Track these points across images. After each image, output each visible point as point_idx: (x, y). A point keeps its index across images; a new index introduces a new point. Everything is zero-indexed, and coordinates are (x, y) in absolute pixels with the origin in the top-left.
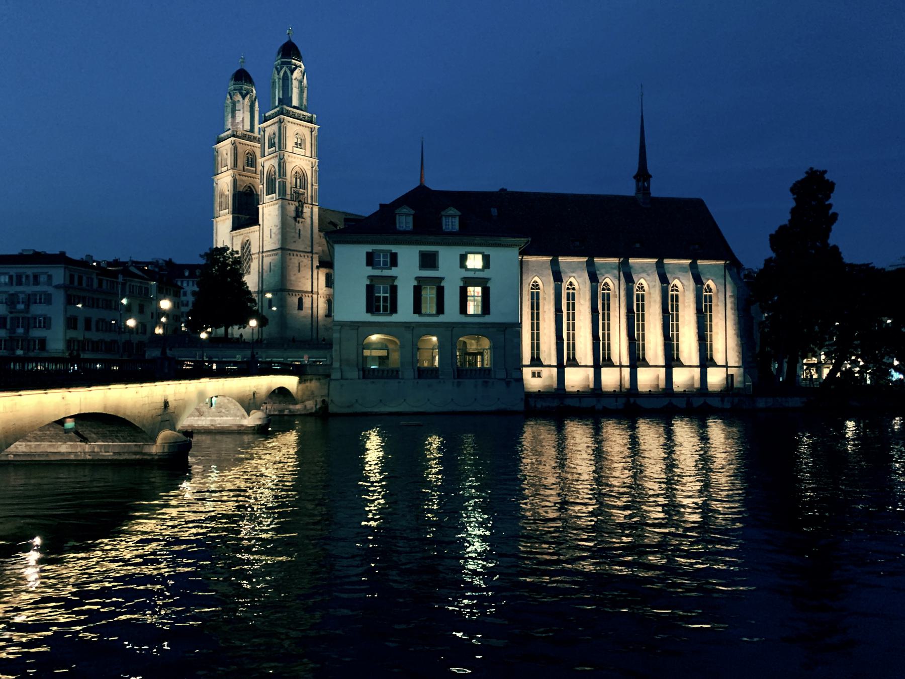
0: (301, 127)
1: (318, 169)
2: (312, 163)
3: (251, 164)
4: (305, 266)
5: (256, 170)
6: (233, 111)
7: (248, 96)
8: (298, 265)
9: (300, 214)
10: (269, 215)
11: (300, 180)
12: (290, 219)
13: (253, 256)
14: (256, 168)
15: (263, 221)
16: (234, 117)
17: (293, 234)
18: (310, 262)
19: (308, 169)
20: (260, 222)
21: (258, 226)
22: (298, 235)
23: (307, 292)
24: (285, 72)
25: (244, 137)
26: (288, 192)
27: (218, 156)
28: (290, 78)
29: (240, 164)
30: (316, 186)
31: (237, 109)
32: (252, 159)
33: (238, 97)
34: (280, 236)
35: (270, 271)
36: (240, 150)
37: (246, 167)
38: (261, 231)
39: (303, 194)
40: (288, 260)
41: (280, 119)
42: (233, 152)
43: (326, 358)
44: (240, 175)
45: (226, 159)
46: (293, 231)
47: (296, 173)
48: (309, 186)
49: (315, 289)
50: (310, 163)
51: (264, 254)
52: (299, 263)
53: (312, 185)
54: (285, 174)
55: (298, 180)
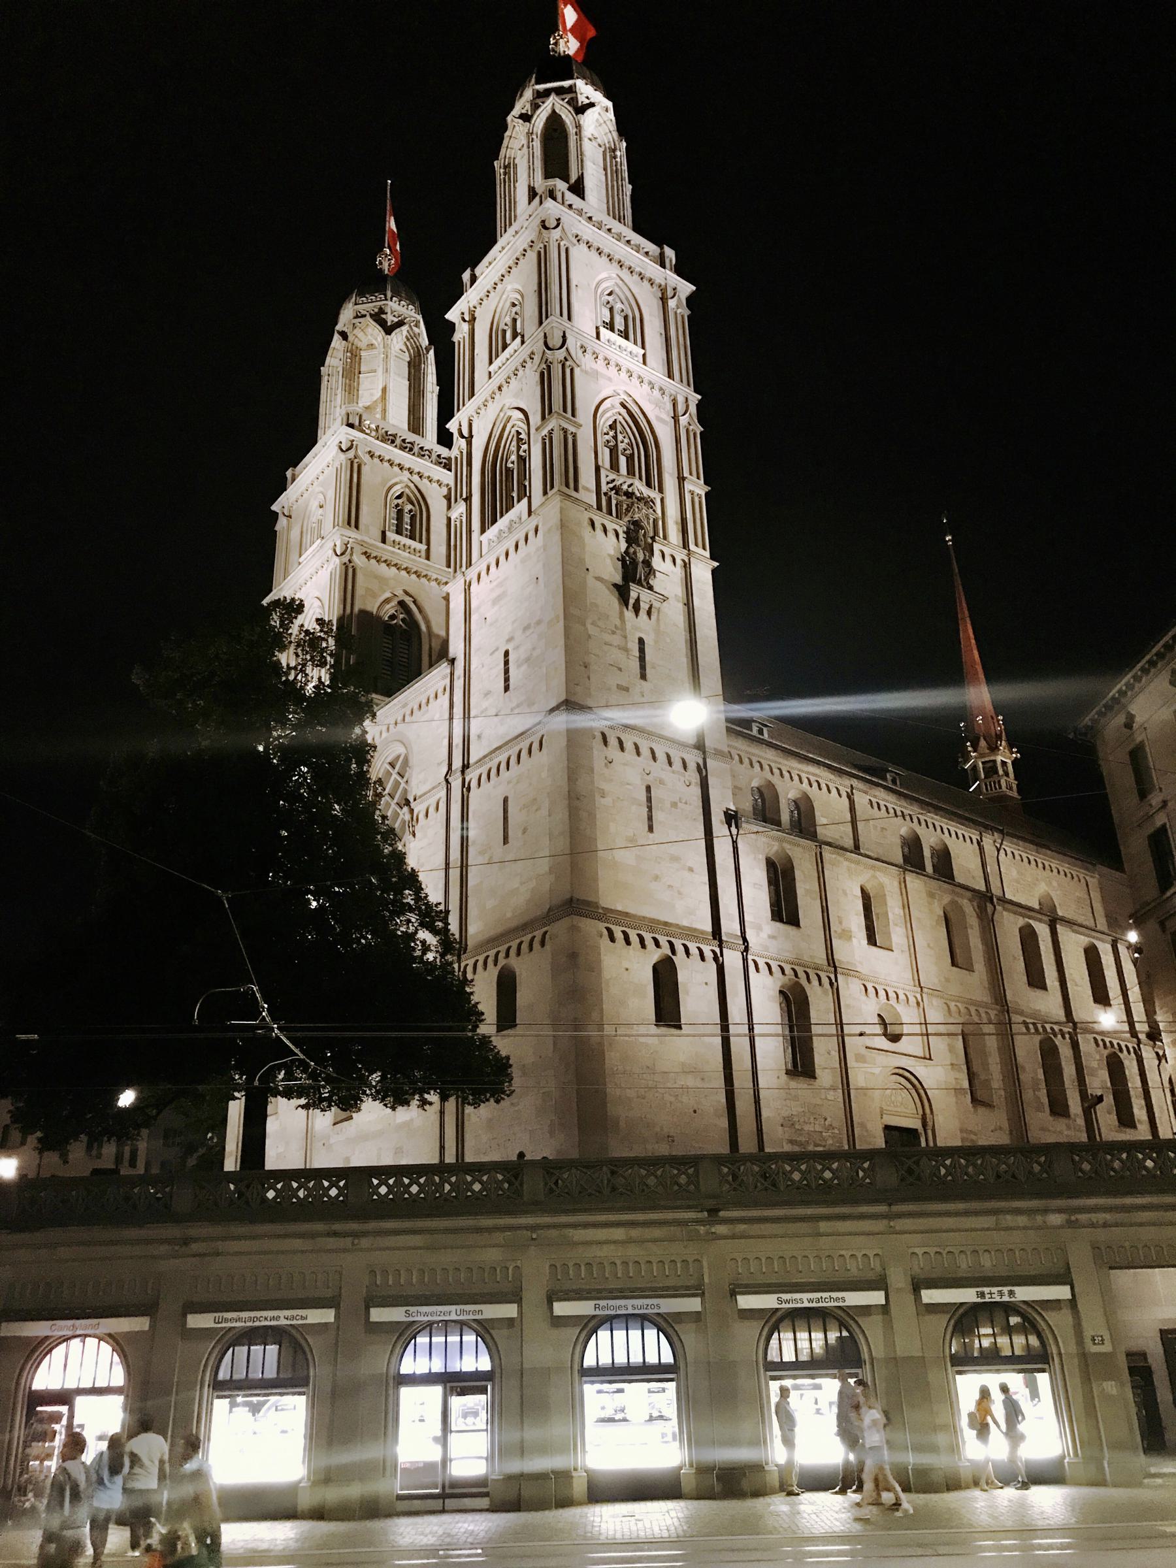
0: (625, 274)
1: (699, 429)
2: (675, 405)
3: (413, 531)
4: (674, 805)
5: (428, 550)
6: (352, 371)
7: (405, 328)
8: (644, 798)
9: (641, 571)
10: (496, 601)
11: (630, 459)
12: (598, 584)
13: (419, 808)
14: (428, 544)
15: (467, 639)
16: (351, 390)
17: (616, 655)
18: (696, 791)
19: (658, 418)
20: (456, 648)
21: (443, 669)
22: (635, 664)
23: (692, 933)
24: (554, 121)
25: (389, 438)
26: (587, 478)
27: (289, 528)
28: (572, 130)
29: (373, 513)
30: (697, 488)
31: (362, 369)
32: (413, 518)
33: (373, 332)
34: (557, 656)
35: (506, 840)
36: (372, 474)
37: (391, 536)
38: (459, 684)
39: (648, 502)
40: (598, 764)
41: (543, 221)
42: (345, 477)
43: (1063, 1278)
44: (367, 555)
45: (320, 522)
46: (616, 640)
47: (613, 427)
48: (670, 483)
49: (730, 925)
50: (667, 399)
51: (472, 775)
52: (648, 789)
53: (681, 479)
54: (570, 407)
55: (623, 461)
